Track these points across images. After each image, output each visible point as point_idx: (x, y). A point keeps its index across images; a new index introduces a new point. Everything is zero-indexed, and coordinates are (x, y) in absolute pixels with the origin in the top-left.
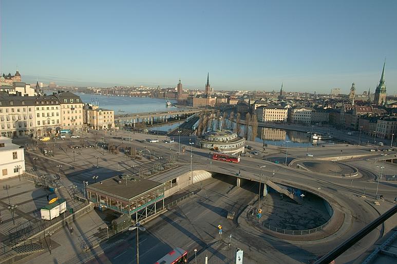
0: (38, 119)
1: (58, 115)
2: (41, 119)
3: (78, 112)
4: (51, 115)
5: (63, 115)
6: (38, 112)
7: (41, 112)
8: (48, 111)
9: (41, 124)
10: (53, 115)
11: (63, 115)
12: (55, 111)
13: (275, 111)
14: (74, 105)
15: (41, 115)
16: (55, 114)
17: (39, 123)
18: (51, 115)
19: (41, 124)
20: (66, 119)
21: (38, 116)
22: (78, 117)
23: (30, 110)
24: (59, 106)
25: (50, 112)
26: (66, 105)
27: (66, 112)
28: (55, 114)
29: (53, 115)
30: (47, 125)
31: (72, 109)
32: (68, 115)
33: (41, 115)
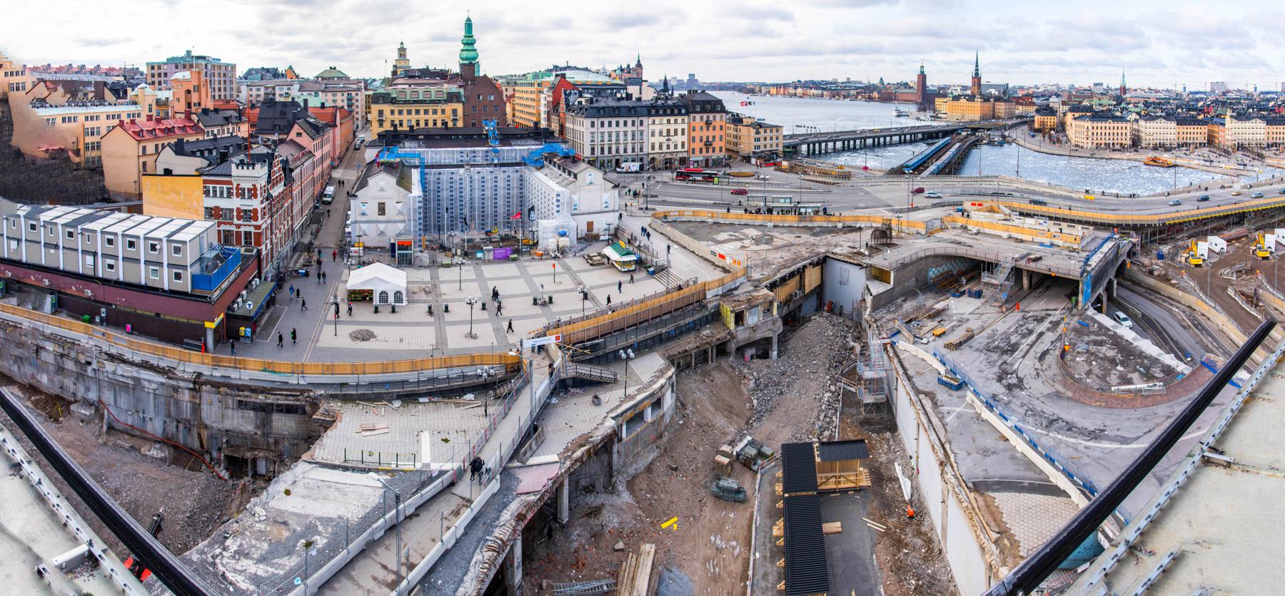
0: (652, 140)
1: (683, 134)
2: (657, 140)
3: (718, 128)
4: (672, 133)
5: (693, 134)
6: (652, 127)
7: (657, 128)
8: (669, 127)
9: (657, 150)
10: (676, 133)
11: (693, 134)
12: (680, 127)
14: (711, 116)
15: (657, 133)
16: (679, 132)
17: (653, 148)
18: (672, 133)
19: (657, 150)
20: (697, 140)
21: (653, 135)
22: (717, 139)
23: (642, 123)
24: (686, 118)
25: (672, 127)
26: (698, 116)
27: (698, 129)
28: (679, 132)
29: (676, 133)
30: (664, 150)
32: (701, 134)
33: (657, 133)
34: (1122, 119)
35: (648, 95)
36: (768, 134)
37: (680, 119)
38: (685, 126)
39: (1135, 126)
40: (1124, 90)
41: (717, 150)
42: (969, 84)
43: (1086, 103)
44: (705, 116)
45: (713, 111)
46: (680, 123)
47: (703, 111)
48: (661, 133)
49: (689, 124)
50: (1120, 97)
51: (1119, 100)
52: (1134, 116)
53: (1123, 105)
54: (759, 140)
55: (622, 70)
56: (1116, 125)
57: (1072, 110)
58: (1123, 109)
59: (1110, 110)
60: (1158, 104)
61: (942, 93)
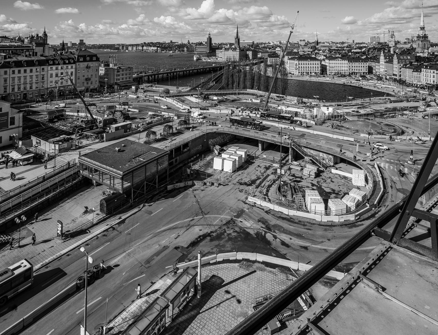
13: (307, 62)
14: (90, 64)
24: (74, 66)
26: (81, 64)
31: (88, 67)
34: (315, 59)
35: (49, 53)
36: (125, 72)
37: (70, 67)
38: (73, 70)
39: (323, 63)
40: (318, 43)
41: (94, 83)
42: (233, 41)
43: (295, 50)
44: (86, 64)
45: (91, 60)
46: (70, 69)
47: (85, 61)
48: (57, 75)
49: (76, 69)
50: (315, 46)
51: (314, 48)
52: (322, 57)
53: (316, 51)
54: (119, 75)
55: (33, 37)
56: (312, 62)
57: (287, 55)
58: (316, 53)
59: (308, 54)
60: (337, 51)
61: (220, 47)
